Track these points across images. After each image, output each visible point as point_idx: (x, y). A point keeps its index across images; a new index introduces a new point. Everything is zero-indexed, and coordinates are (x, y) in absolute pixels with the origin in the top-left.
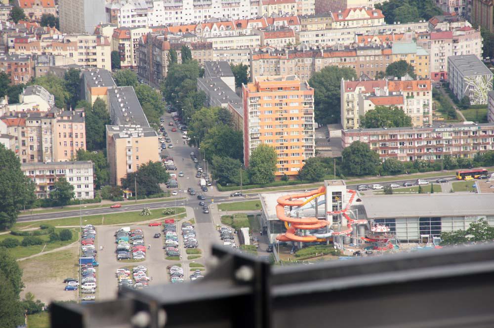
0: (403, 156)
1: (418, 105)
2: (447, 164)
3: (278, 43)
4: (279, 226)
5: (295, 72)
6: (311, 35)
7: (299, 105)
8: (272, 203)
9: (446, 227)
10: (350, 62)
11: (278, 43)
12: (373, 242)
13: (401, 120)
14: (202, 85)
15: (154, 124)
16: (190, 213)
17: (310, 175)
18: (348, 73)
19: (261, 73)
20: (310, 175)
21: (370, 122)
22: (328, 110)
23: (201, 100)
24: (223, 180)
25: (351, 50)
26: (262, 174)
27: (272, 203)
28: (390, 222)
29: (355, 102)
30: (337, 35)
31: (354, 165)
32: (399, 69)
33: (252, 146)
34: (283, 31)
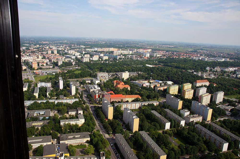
0: (44, 68)
1: (45, 65)
2: (47, 69)
3: (34, 60)
4: (35, 73)
5: (36, 62)
6: (37, 60)
7: (37, 65)
8: (35, 71)
9: (47, 73)
10: (40, 62)
11: (34, 60)
12: (42, 74)
13: (44, 66)
14: (29, 63)
15: (25, 66)
16: (29, 72)
17: (37, 69)
18: (40, 62)
19: (33, 62)
20: (37, 69)
21: (41, 66)
22: (38, 65)
23: (29, 64)
24: (31, 70)
25: (40, 61)
26: (34, 69)
27: (35, 71)
28: (43, 72)
29: (40, 64)
30: (39, 60)
31: (41, 69)
32: (43, 62)
33: (33, 67)
34: (35, 59)
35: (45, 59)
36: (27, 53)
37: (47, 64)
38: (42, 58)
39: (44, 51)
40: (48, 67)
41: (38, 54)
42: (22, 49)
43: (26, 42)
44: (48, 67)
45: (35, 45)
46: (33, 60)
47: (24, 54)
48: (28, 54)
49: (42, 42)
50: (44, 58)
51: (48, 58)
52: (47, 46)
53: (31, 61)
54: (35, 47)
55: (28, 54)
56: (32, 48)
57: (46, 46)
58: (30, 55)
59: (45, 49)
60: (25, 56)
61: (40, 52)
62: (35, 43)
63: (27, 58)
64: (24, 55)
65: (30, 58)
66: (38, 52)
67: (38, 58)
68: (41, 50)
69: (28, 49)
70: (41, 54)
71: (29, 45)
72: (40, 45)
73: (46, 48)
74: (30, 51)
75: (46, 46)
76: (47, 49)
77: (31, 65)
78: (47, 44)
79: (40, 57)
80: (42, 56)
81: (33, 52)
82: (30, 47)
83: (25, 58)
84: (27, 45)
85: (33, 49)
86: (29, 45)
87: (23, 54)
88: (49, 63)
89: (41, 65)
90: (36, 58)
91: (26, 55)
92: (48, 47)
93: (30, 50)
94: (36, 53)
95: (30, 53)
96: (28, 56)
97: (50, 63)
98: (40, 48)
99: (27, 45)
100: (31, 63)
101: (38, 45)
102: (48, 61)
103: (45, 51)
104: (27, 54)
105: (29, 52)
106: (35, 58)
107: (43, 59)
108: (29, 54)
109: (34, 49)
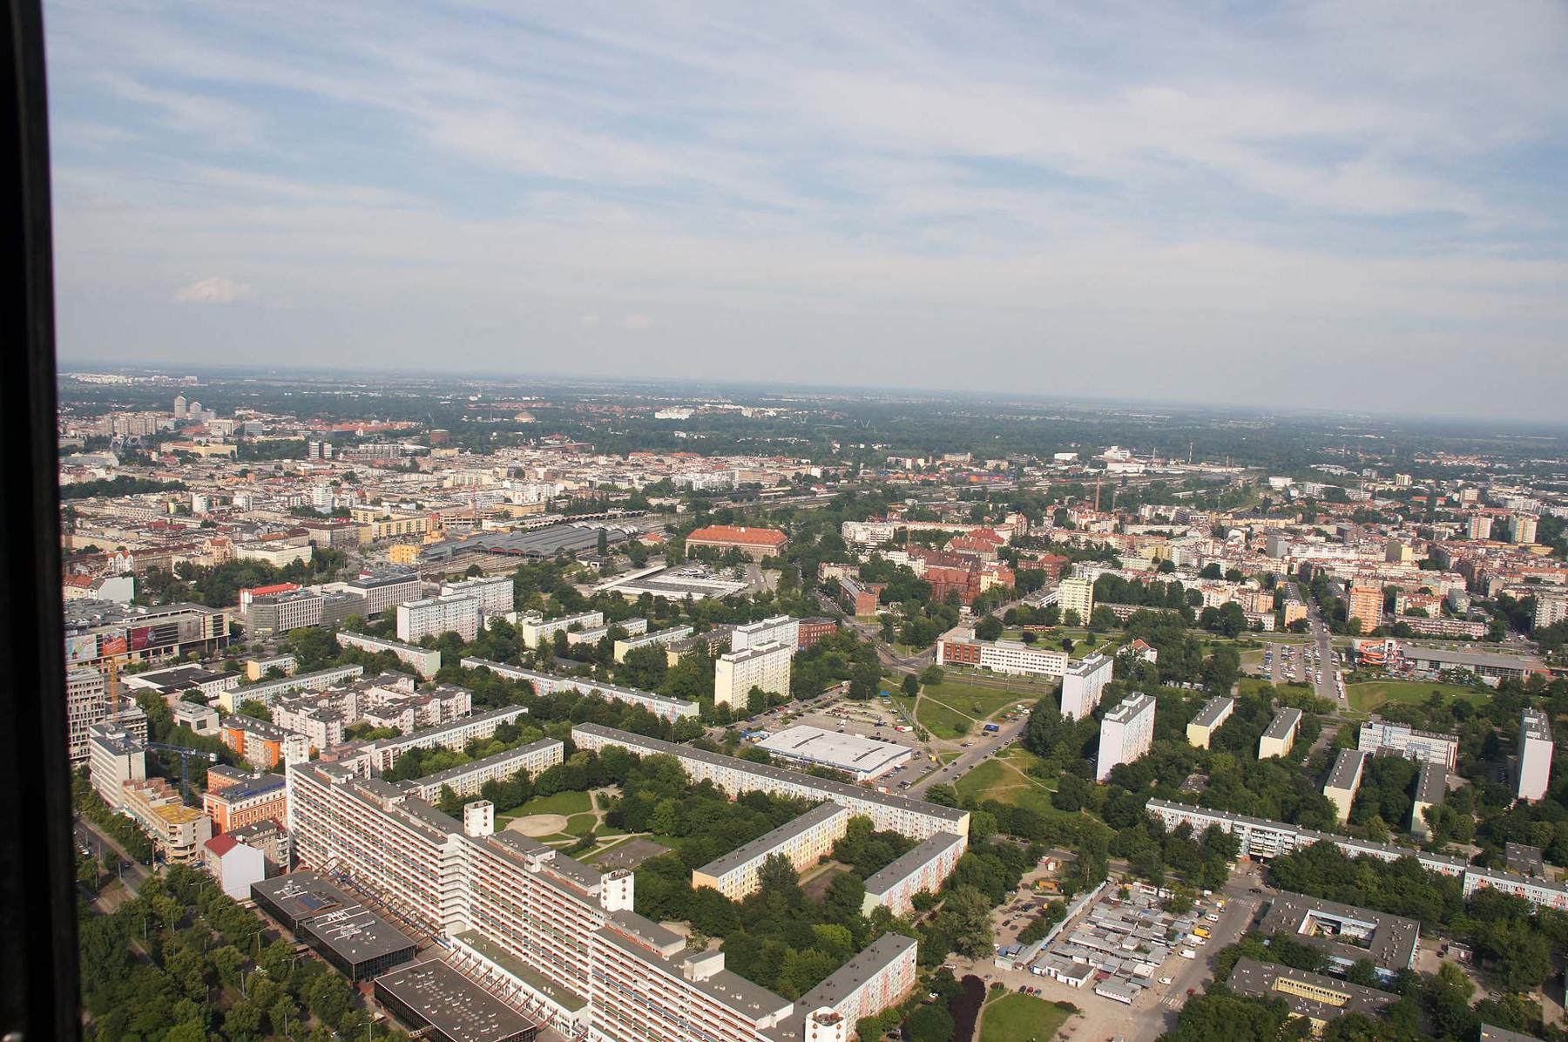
0: (1423, 631)
1: (1433, 608)
2: (1445, 637)
3: (1368, 572)
4: (1361, 655)
6: (1384, 570)
7: (1376, 601)
8: (1358, 643)
9: (1442, 666)
10: (1401, 584)
11: (1368, 572)
12: (1406, 669)
13: (1425, 615)
15: (1304, 602)
16: (1318, 643)
17: (1377, 634)
18: (1400, 589)
19: (1357, 584)
20: (1377, 634)
21: (1408, 613)
22: (1389, 606)
23: (1329, 593)
24: (1334, 631)
26: (1354, 629)
27: (1358, 643)
28: (1415, 660)
29: (1402, 603)
30: (1396, 571)
31: (1400, 632)
32: (1425, 591)
33: (1351, 616)
34: (1369, 567)
35: (1438, 573)
36: (1327, 523)
37: (1448, 606)
38: (1422, 565)
39: (1439, 517)
40: (1451, 626)
41: (1395, 534)
42: (1302, 492)
43: (1332, 451)
44: (1451, 626)
45: (1388, 474)
46: (1356, 570)
47: (1305, 527)
48: (1331, 530)
49: (1434, 457)
50: (1435, 561)
51: (1464, 568)
52: (1465, 487)
53: (1342, 571)
54: (1387, 485)
55: (1331, 530)
56: (1366, 490)
57: (1460, 482)
58: (1341, 538)
59: (1450, 502)
60: (1311, 538)
61: (1411, 524)
62: (1385, 461)
63: (1325, 554)
64: (1309, 533)
65: (1339, 554)
66: (1400, 518)
67: (1393, 557)
68: (1418, 511)
69: (1335, 495)
70: (1420, 533)
71: (1345, 472)
72: (1417, 474)
73: (1456, 497)
74: (1350, 513)
75: (1460, 482)
76: (1465, 505)
77: (1339, 602)
78: (1471, 469)
79: (1407, 553)
80: (1424, 547)
81: (1367, 519)
82: (1354, 486)
83: (1311, 553)
84: (1337, 471)
85: (1369, 495)
86: (1345, 472)
87: (1302, 523)
88: (1463, 604)
89: (1409, 606)
90: (1382, 556)
91: (1319, 533)
92: (1471, 494)
93: (1347, 501)
94: (1383, 527)
95: (1345, 525)
96: (1329, 539)
97: (1473, 604)
98: (1418, 493)
99: (1337, 471)
100: (1342, 586)
101: (1407, 477)
102: (1461, 585)
103: (1447, 518)
104: (1324, 528)
105: (1338, 518)
106: (1372, 557)
107: (1426, 572)
108: (1340, 531)
109: (1373, 498)
